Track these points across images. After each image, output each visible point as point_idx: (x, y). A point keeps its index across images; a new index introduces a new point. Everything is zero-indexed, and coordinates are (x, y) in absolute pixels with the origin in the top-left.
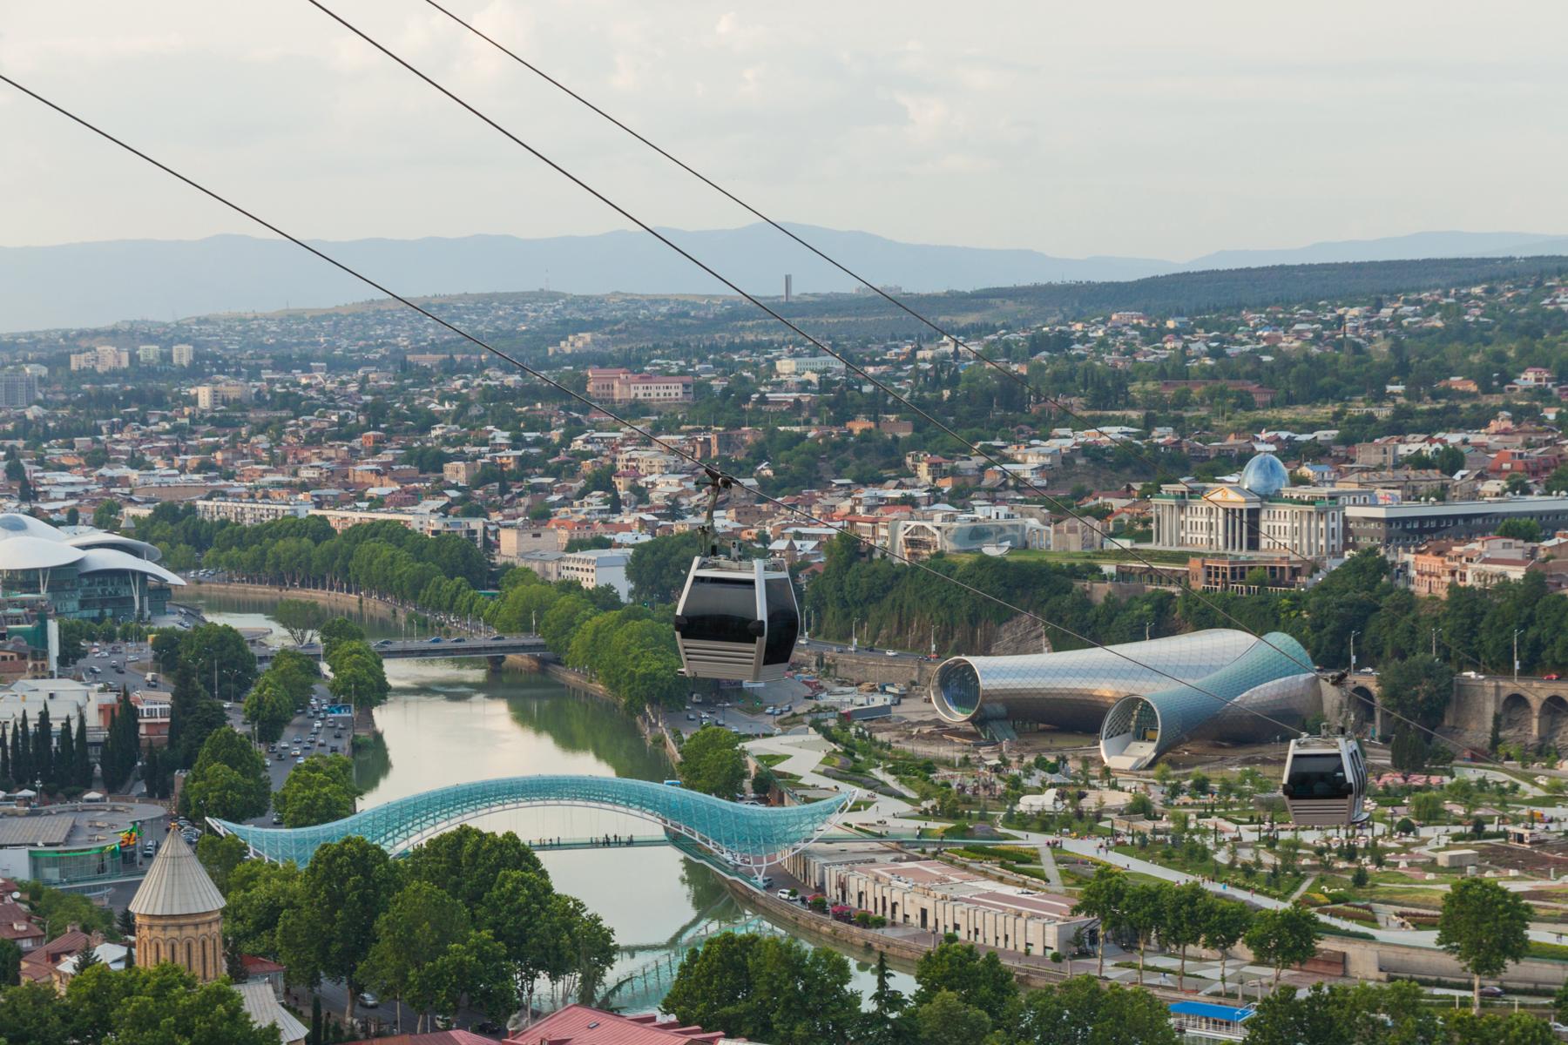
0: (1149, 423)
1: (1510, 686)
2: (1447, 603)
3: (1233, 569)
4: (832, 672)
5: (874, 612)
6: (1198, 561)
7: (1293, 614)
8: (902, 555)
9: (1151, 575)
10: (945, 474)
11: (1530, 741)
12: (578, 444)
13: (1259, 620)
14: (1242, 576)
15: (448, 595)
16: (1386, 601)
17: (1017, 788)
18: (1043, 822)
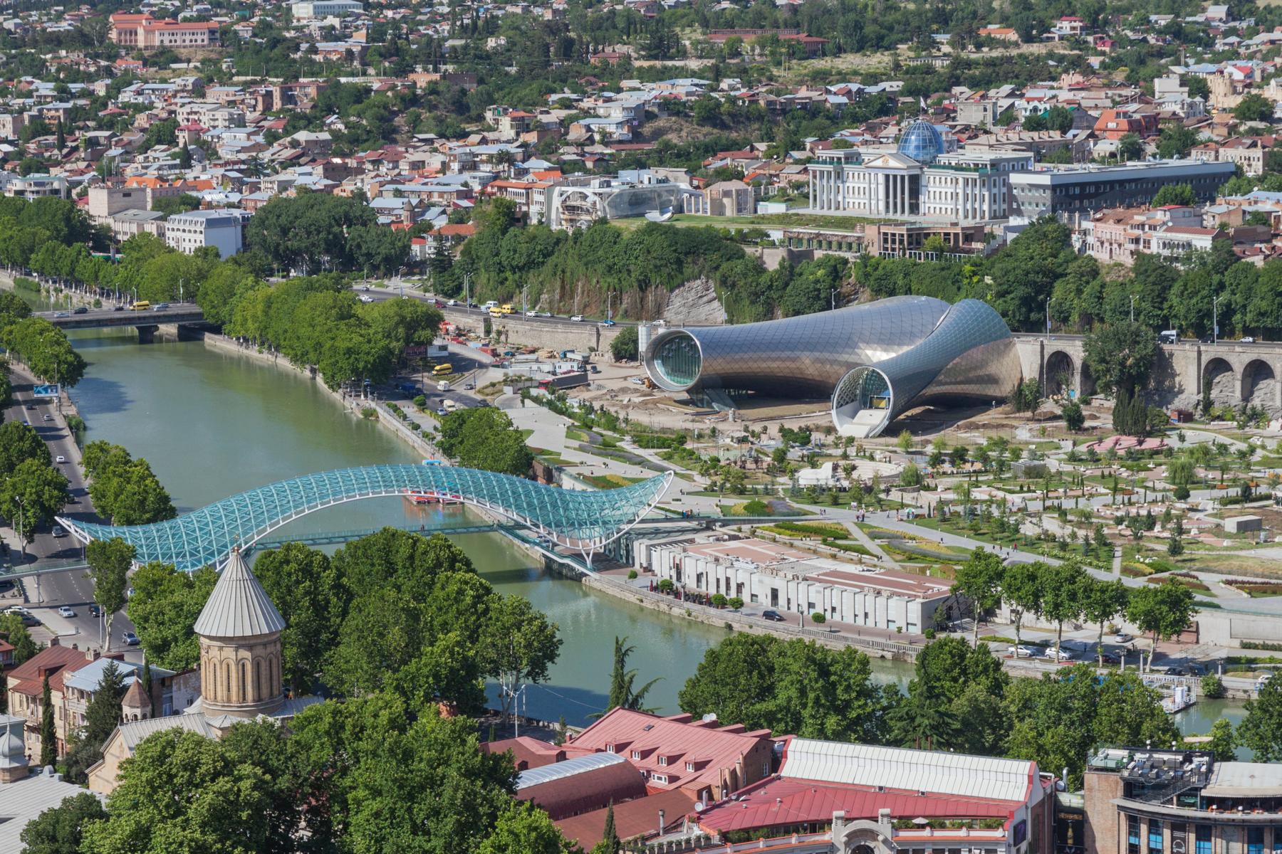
0: (718, 74)
1: (1212, 351)
2: (1136, 269)
3: (910, 236)
4: (503, 338)
5: (533, 278)
6: (875, 228)
7: (975, 279)
8: (558, 223)
9: (820, 241)
10: (527, 129)
11: (1233, 403)
12: (127, 96)
13: (947, 284)
14: (919, 243)
15: (68, 262)
16: (1072, 267)
17: (781, 464)
18: (835, 497)
